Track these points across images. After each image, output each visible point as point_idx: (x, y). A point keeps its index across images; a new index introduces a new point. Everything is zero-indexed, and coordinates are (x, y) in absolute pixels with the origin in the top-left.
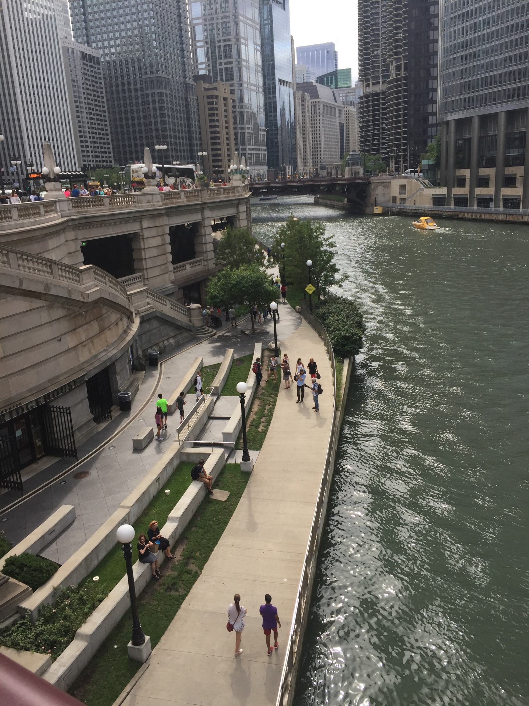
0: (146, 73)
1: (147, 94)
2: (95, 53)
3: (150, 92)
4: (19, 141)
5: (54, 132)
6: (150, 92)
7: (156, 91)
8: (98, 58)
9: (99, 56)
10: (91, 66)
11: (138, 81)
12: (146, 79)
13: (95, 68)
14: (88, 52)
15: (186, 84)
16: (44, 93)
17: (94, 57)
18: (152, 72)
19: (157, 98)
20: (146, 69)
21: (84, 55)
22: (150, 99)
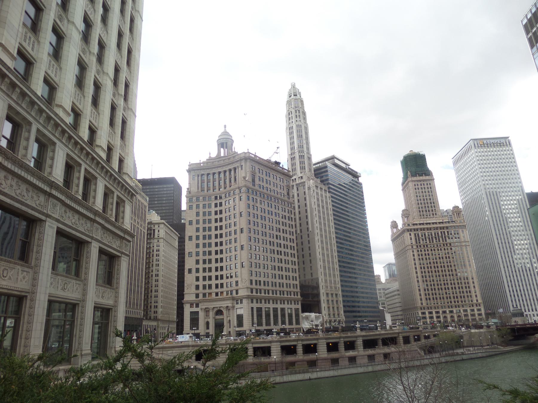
5: (532, 285)
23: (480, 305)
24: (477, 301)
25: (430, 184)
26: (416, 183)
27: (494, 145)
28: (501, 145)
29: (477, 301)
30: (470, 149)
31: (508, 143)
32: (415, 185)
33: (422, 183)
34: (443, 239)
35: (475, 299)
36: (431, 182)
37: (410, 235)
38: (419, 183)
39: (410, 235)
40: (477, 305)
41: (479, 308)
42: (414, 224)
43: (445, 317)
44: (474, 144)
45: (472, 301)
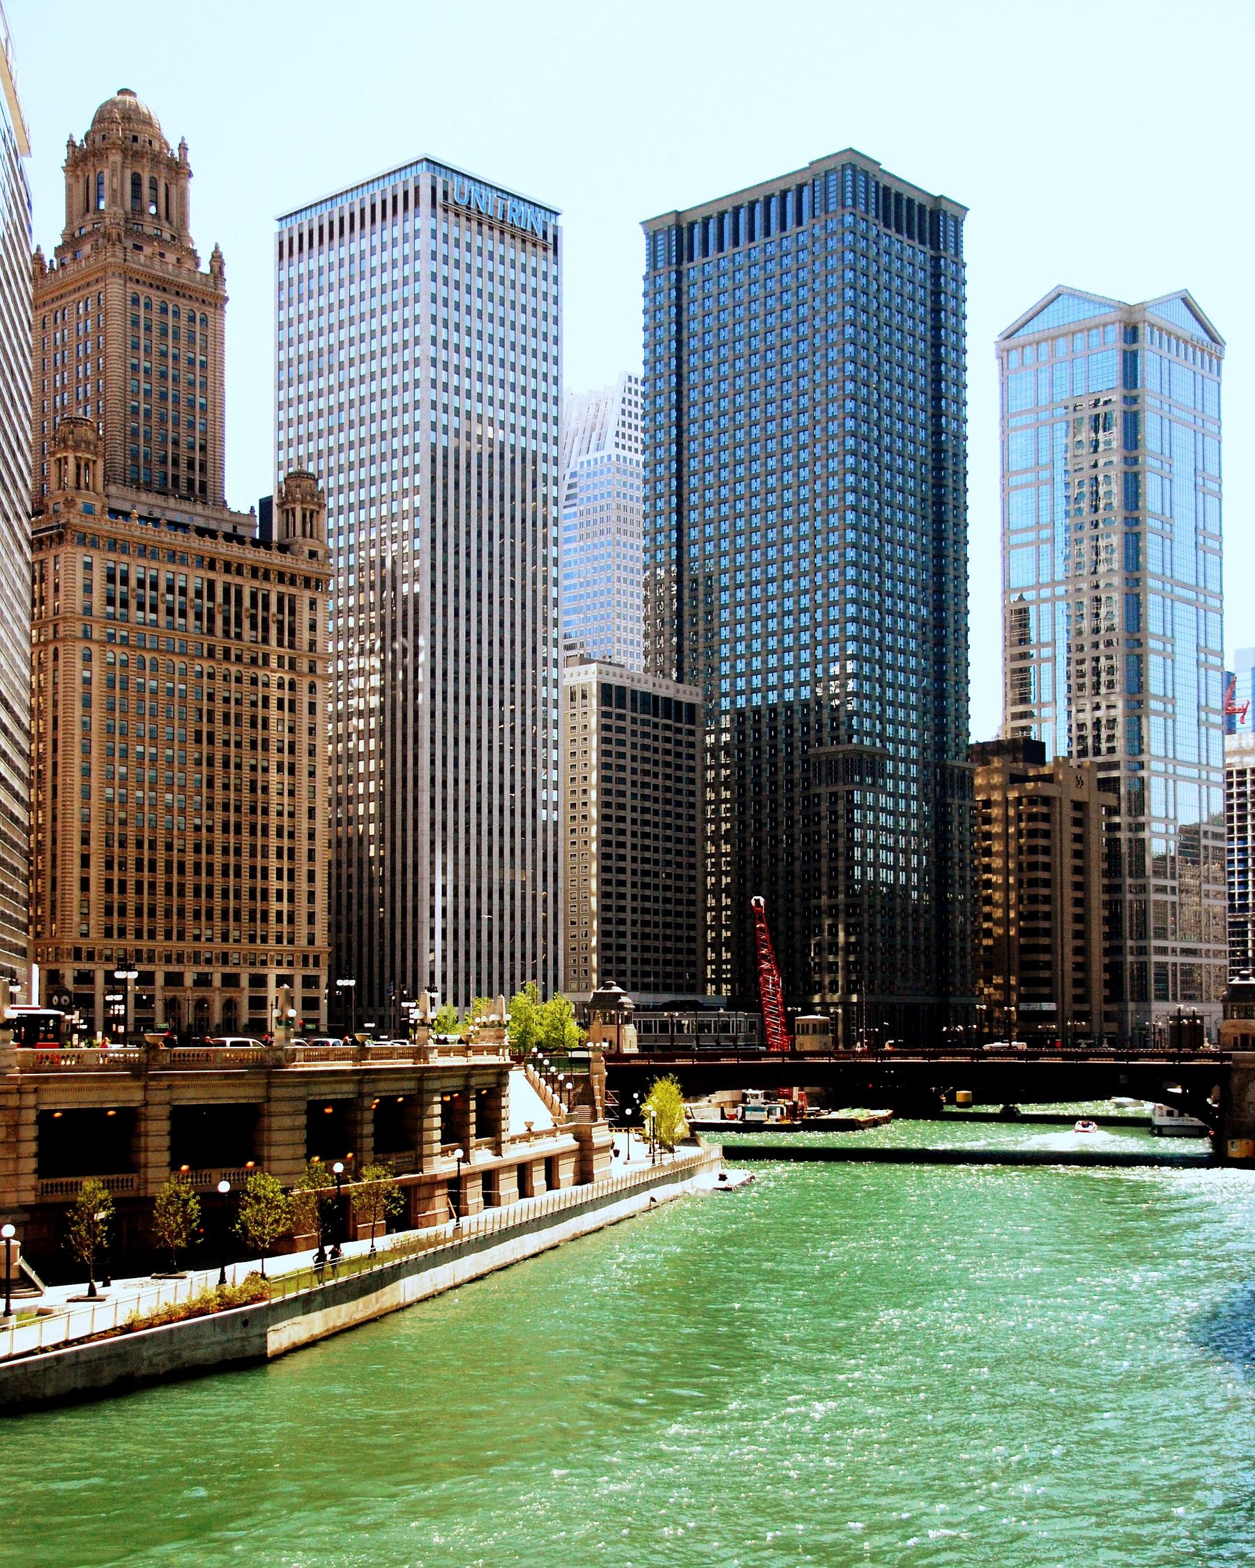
0: (820, 741)
1: (818, 796)
2: (688, 694)
3: (823, 790)
4: (410, 919)
5: (507, 898)
6: (823, 790)
7: (841, 788)
8: (691, 707)
9: (698, 700)
10: (667, 727)
11: (797, 762)
12: (817, 756)
13: (679, 731)
14: (662, 693)
15: (943, 768)
16: (496, 803)
17: (679, 704)
18: (835, 739)
19: (841, 807)
20: (820, 730)
21: (649, 702)
22: (824, 806)
23: (316, 964)
24: (311, 941)
25: (204, 321)
26: (144, 292)
27: (503, 228)
28: (525, 238)
29: (311, 941)
30: (403, 202)
31: (550, 239)
32: (136, 301)
33: (172, 302)
34: (226, 621)
35: (303, 930)
36: (209, 310)
37: (88, 566)
38: (156, 297)
39: (88, 566)
40: (305, 964)
41: (311, 971)
42: (114, 513)
43: (201, 1004)
44: (434, 190)
45: (291, 941)
